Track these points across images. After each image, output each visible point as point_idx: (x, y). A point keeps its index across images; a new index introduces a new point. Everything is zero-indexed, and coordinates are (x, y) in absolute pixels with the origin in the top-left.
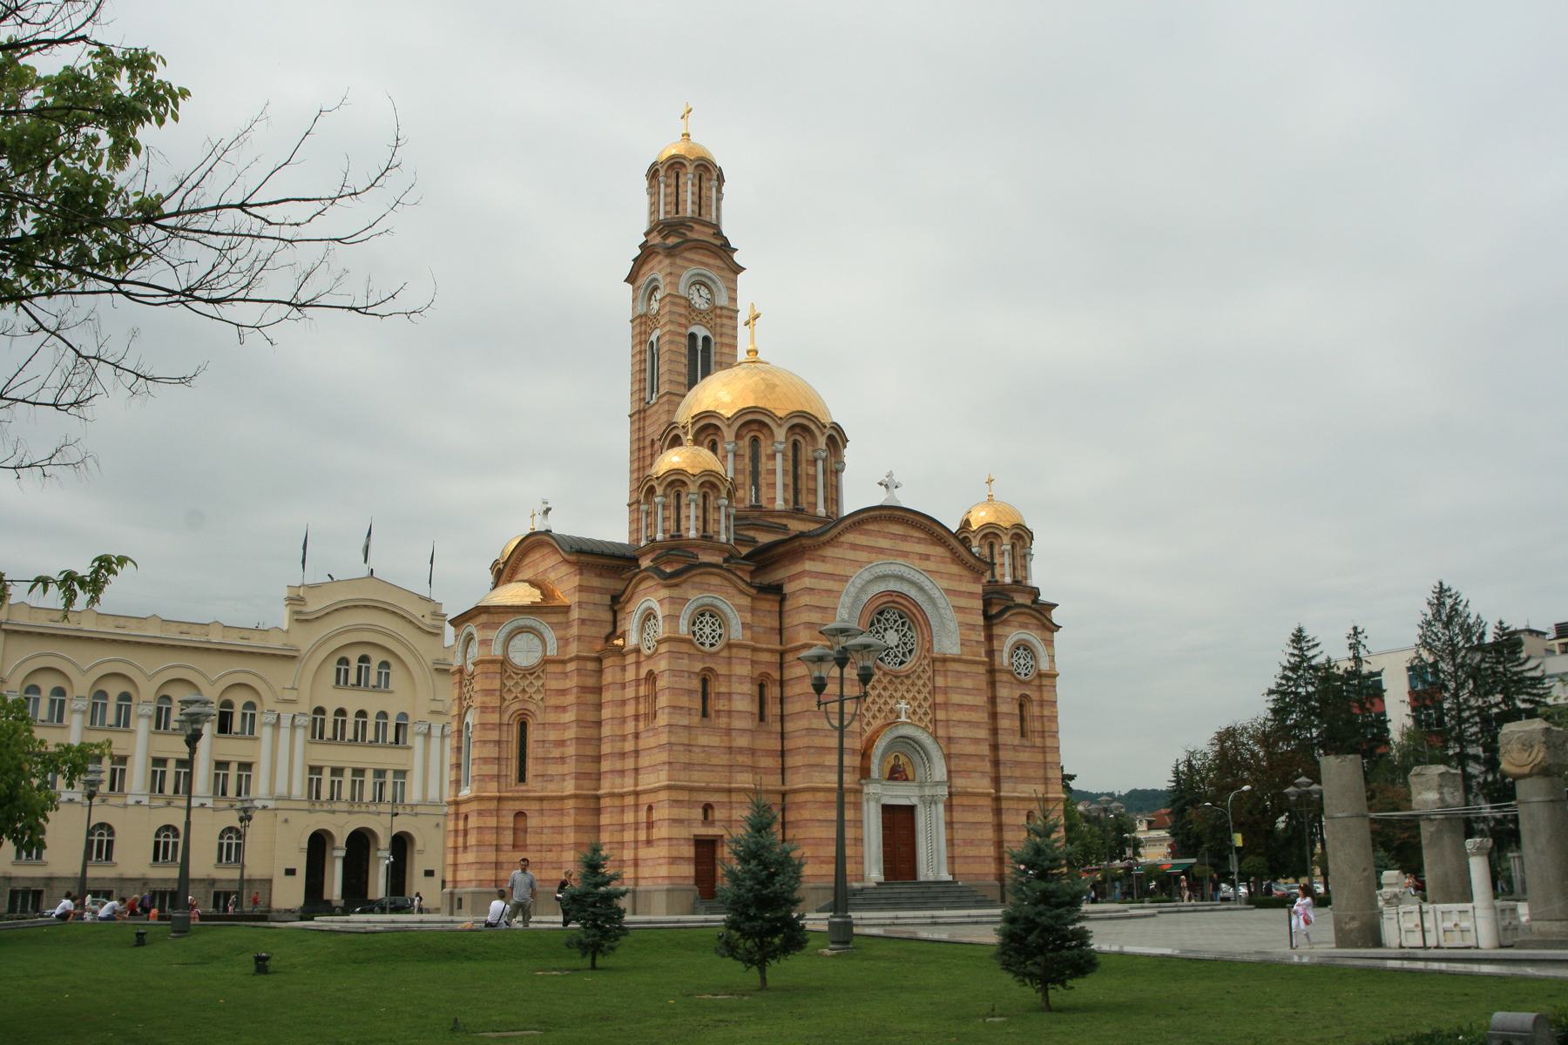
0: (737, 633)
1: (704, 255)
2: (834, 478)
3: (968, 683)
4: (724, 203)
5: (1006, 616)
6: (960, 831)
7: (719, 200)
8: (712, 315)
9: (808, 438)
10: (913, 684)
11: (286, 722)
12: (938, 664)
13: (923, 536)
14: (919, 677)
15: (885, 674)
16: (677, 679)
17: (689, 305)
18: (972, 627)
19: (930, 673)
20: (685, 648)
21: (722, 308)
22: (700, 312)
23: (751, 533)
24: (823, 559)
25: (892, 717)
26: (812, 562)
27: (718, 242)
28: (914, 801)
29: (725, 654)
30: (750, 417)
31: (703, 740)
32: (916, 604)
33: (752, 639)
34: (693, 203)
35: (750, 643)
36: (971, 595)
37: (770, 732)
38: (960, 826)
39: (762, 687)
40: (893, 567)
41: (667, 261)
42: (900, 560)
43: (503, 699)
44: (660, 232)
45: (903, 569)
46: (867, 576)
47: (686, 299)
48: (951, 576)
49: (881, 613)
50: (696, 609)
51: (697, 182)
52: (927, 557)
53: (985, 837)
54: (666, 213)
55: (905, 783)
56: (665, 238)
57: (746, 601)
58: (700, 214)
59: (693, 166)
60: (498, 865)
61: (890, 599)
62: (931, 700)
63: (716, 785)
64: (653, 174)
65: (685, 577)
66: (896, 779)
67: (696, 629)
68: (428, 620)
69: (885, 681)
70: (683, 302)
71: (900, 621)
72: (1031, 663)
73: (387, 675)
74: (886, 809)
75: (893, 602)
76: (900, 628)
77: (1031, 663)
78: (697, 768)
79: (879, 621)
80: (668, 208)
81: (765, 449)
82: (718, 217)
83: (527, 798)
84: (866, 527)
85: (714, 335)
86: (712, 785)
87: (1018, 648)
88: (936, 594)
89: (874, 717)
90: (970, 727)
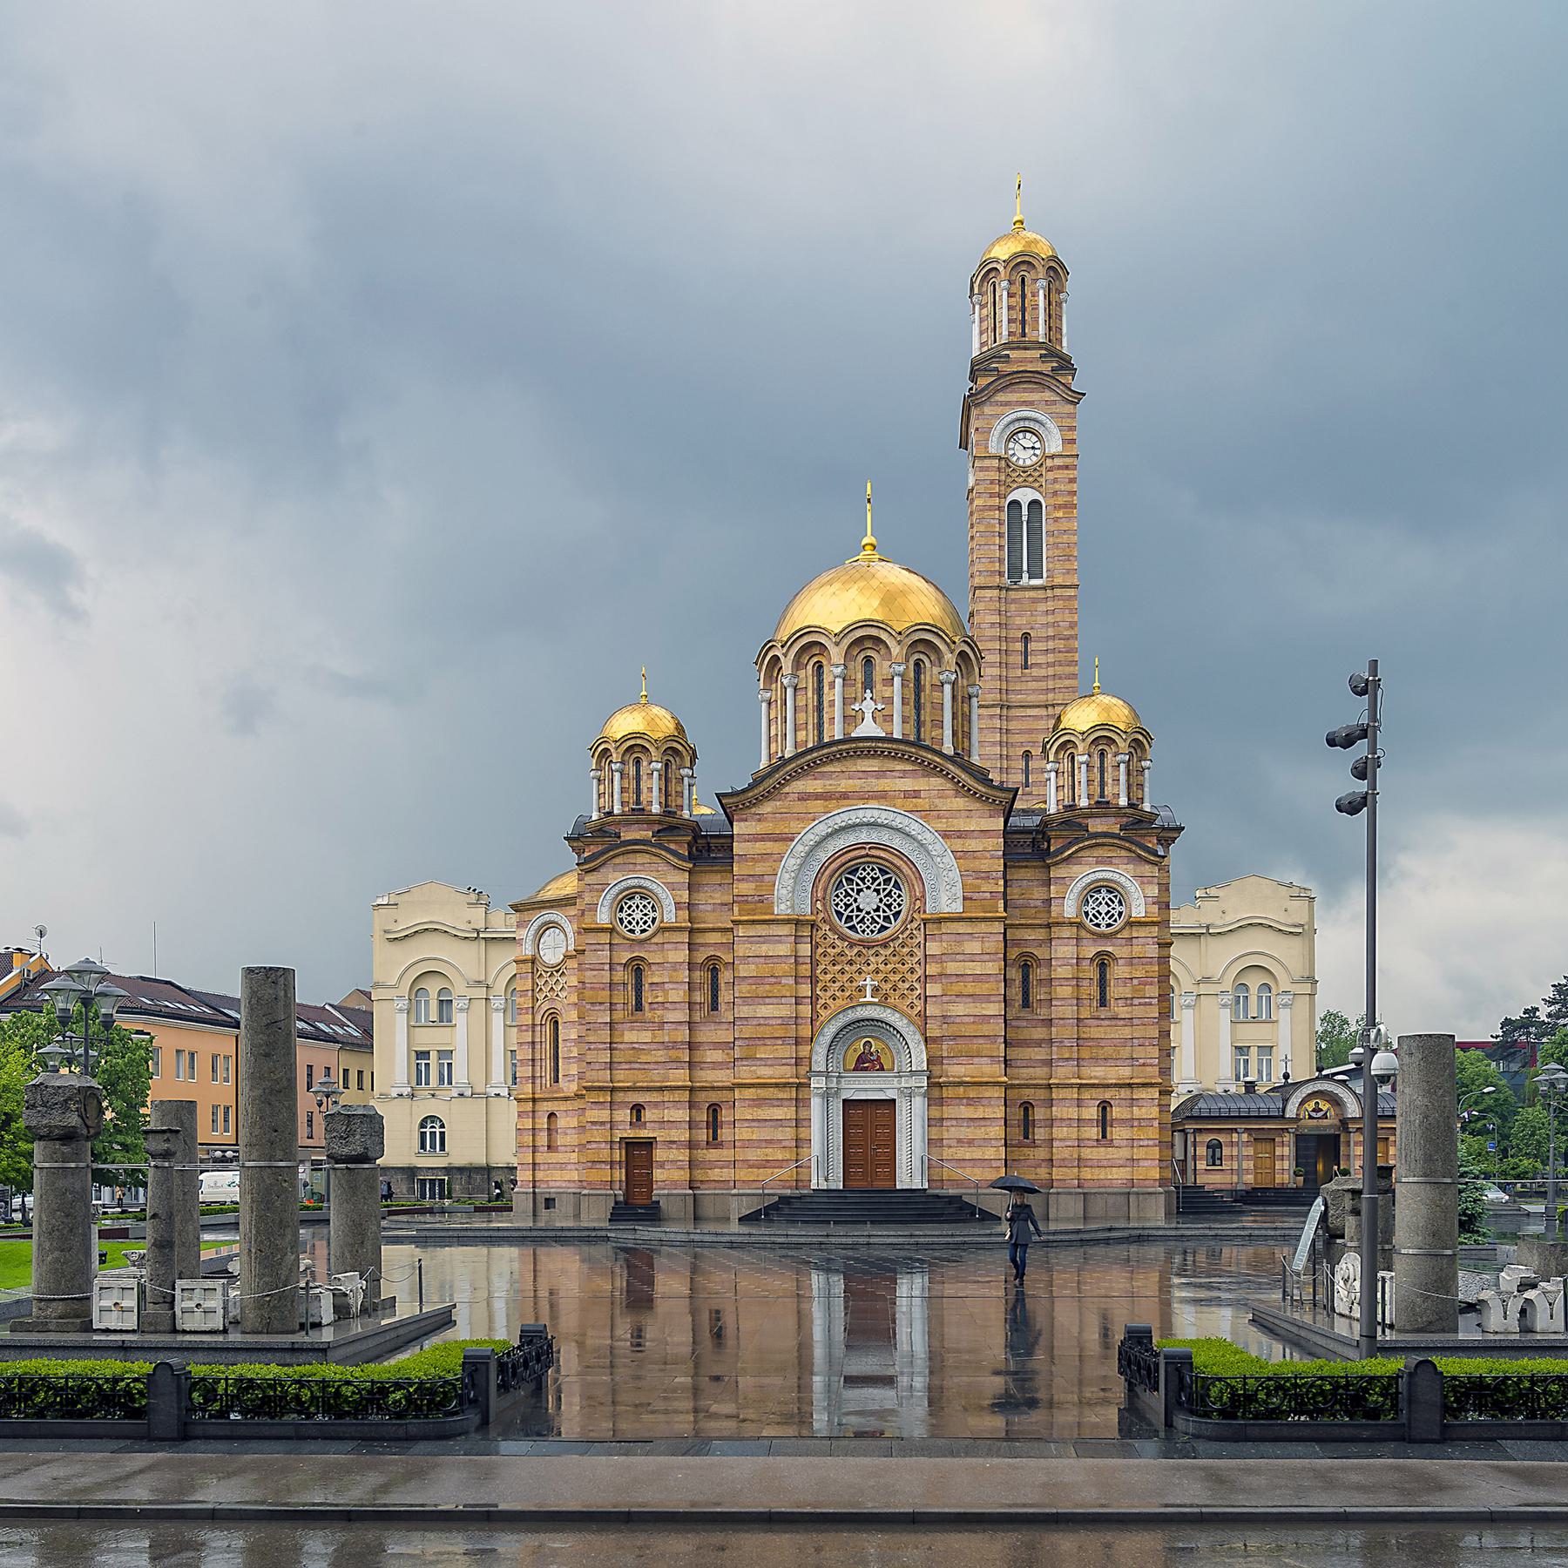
0: (670, 916)
3: (974, 947)
6: (953, 1129)
13: (909, 767)
15: (851, 945)
16: (595, 973)
18: (986, 875)
20: (605, 938)
21: (1052, 457)
22: (1024, 469)
28: (891, 1095)
31: (630, 1036)
35: (683, 925)
38: (954, 1123)
40: (869, 813)
45: (876, 813)
46: (822, 830)
47: (1000, 458)
49: (854, 872)
50: (618, 895)
53: (992, 1135)
61: (863, 852)
62: (920, 972)
66: (866, 1069)
67: (623, 915)
69: (851, 953)
70: (995, 463)
72: (1119, 909)
75: (867, 855)
77: (1119, 909)
83: (556, 1099)
87: (1099, 892)
88: (927, 838)
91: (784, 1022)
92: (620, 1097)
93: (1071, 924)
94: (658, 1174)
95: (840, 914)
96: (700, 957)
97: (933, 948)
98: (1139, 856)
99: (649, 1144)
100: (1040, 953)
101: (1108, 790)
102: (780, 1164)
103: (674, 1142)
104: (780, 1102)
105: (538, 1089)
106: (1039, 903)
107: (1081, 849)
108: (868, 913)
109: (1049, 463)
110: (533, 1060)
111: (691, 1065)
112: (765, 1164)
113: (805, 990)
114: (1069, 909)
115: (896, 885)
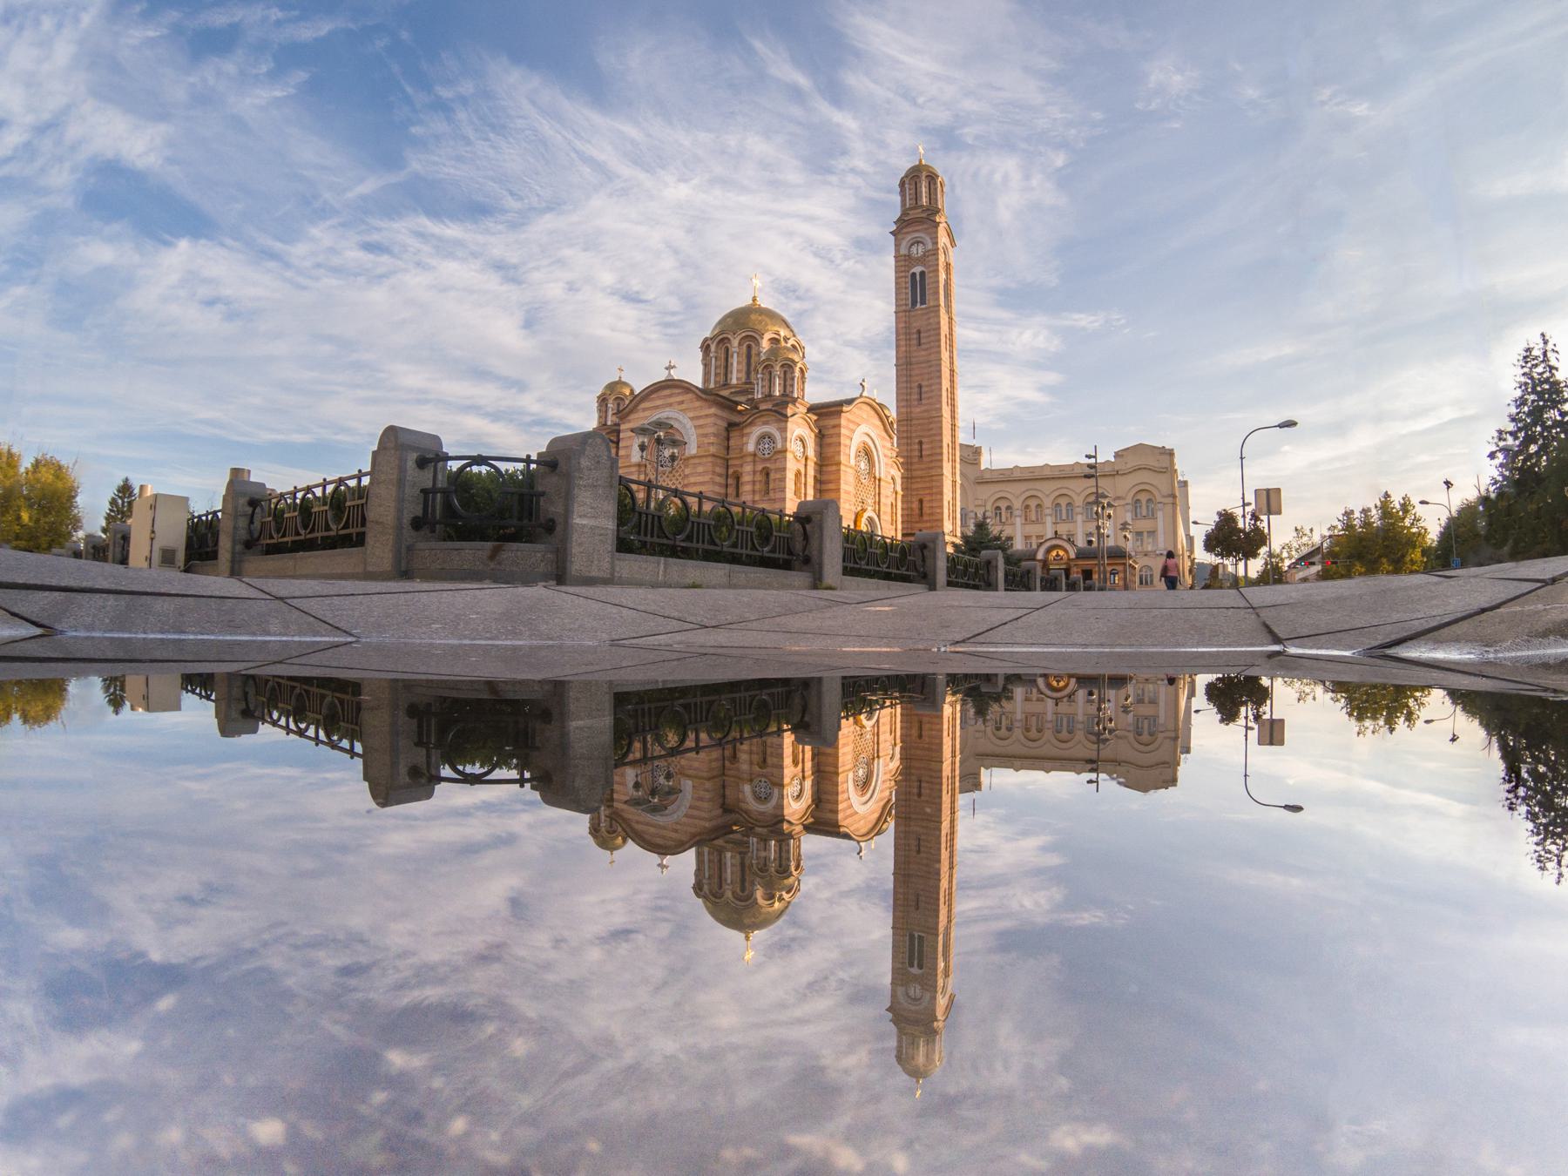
3: (700, 469)
10: (674, 476)
13: (680, 391)
14: (677, 471)
17: (908, 257)
18: (706, 435)
22: (918, 259)
24: (629, 421)
27: (924, 215)
34: (910, 199)
42: (667, 409)
47: (905, 256)
48: (695, 409)
51: (913, 187)
58: (916, 203)
84: (653, 396)
93: (750, 455)
97: (687, 471)
100: (740, 470)
107: (756, 418)
114: (751, 447)
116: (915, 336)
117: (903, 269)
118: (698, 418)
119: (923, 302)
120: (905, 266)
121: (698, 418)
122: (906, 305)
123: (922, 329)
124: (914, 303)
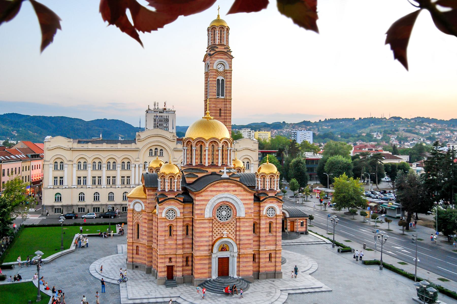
0: (179, 215)
1: (221, 55)
2: (226, 152)
3: (247, 224)
4: (230, 36)
5: (265, 201)
7: (228, 36)
8: (224, 73)
9: (216, 144)
11: (137, 166)
12: (237, 220)
13: (234, 185)
14: (232, 223)
15: (221, 224)
18: (250, 208)
19: (235, 222)
20: (164, 220)
21: (227, 70)
22: (221, 72)
23: (197, 174)
24: (202, 196)
25: (222, 235)
26: (198, 197)
27: (225, 50)
28: (228, 256)
29: (175, 220)
30: (199, 140)
31: (169, 242)
32: (232, 204)
33: (183, 216)
34: (218, 39)
36: (250, 199)
37: (189, 238)
39: (187, 226)
41: (210, 59)
42: (226, 193)
43: (133, 219)
44: (209, 49)
45: (227, 195)
47: (216, 70)
48: (243, 195)
49: (221, 207)
52: (235, 191)
54: (211, 43)
55: (225, 252)
56: (210, 51)
57: (182, 206)
58: (221, 42)
59: (218, 28)
60: (133, 258)
62: (235, 229)
63: (172, 253)
64: (208, 30)
65: (163, 203)
66: (223, 251)
67: (168, 214)
68: (172, 138)
69: (221, 226)
70: (215, 71)
71: (227, 208)
73: (162, 152)
74: (219, 258)
76: (227, 210)
78: (167, 249)
79: (220, 209)
80: (212, 41)
81: (203, 149)
82: (227, 41)
85: (225, 79)
86: (171, 253)
88: (237, 200)
89: (217, 235)
90: (247, 236)
91: (206, 241)
92: (166, 256)
94: (174, 273)
95: (218, 216)
96: (185, 223)
98: (279, 202)
99: (172, 267)
101: (272, 186)
102: (205, 273)
103: (179, 266)
104: (205, 259)
105: (134, 240)
106: (257, 211)
108: (224, 216)
109: (226, 71)
110: (132, 233)
111: (183, 248)
112: (202, 273)
113: (211, 234)
115: (230, 210)
116: (219, 111)
117: (215, 77)
118: (245, 200)
119: (223, 95)
120: (216, 75)
121: (245, 200)
122: (215, 95)
123: (222, 109)
124: (218, 95)
